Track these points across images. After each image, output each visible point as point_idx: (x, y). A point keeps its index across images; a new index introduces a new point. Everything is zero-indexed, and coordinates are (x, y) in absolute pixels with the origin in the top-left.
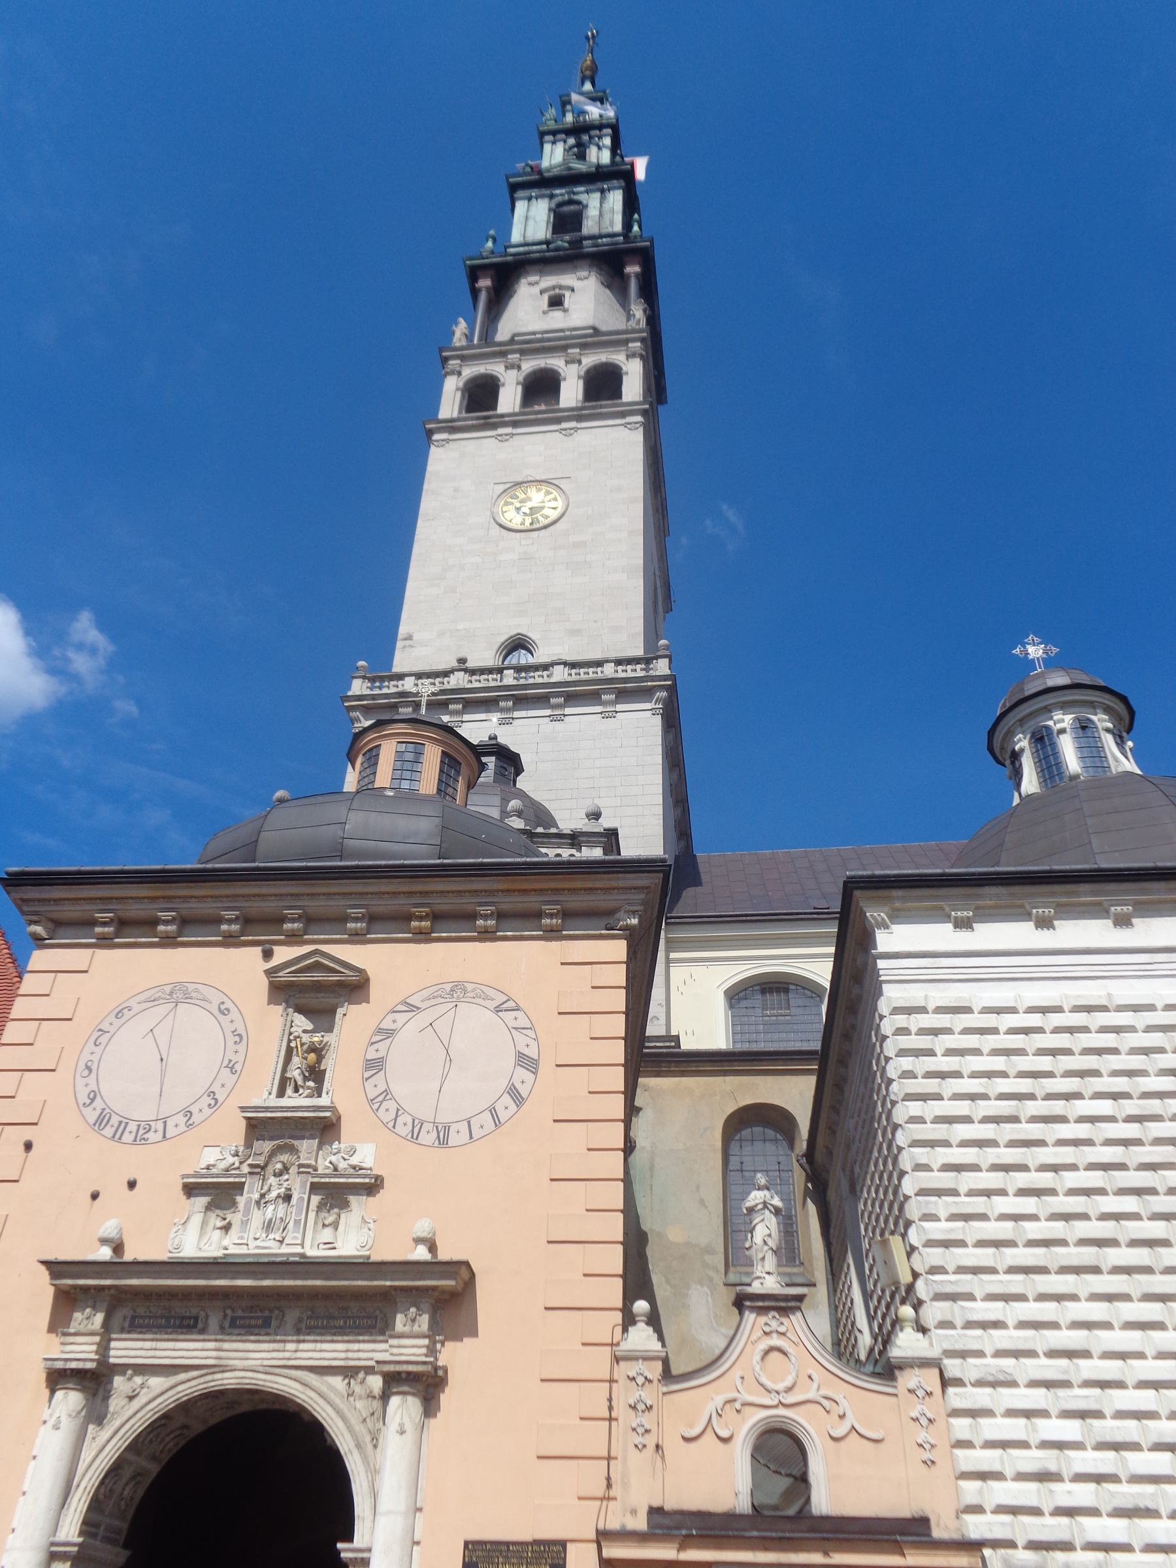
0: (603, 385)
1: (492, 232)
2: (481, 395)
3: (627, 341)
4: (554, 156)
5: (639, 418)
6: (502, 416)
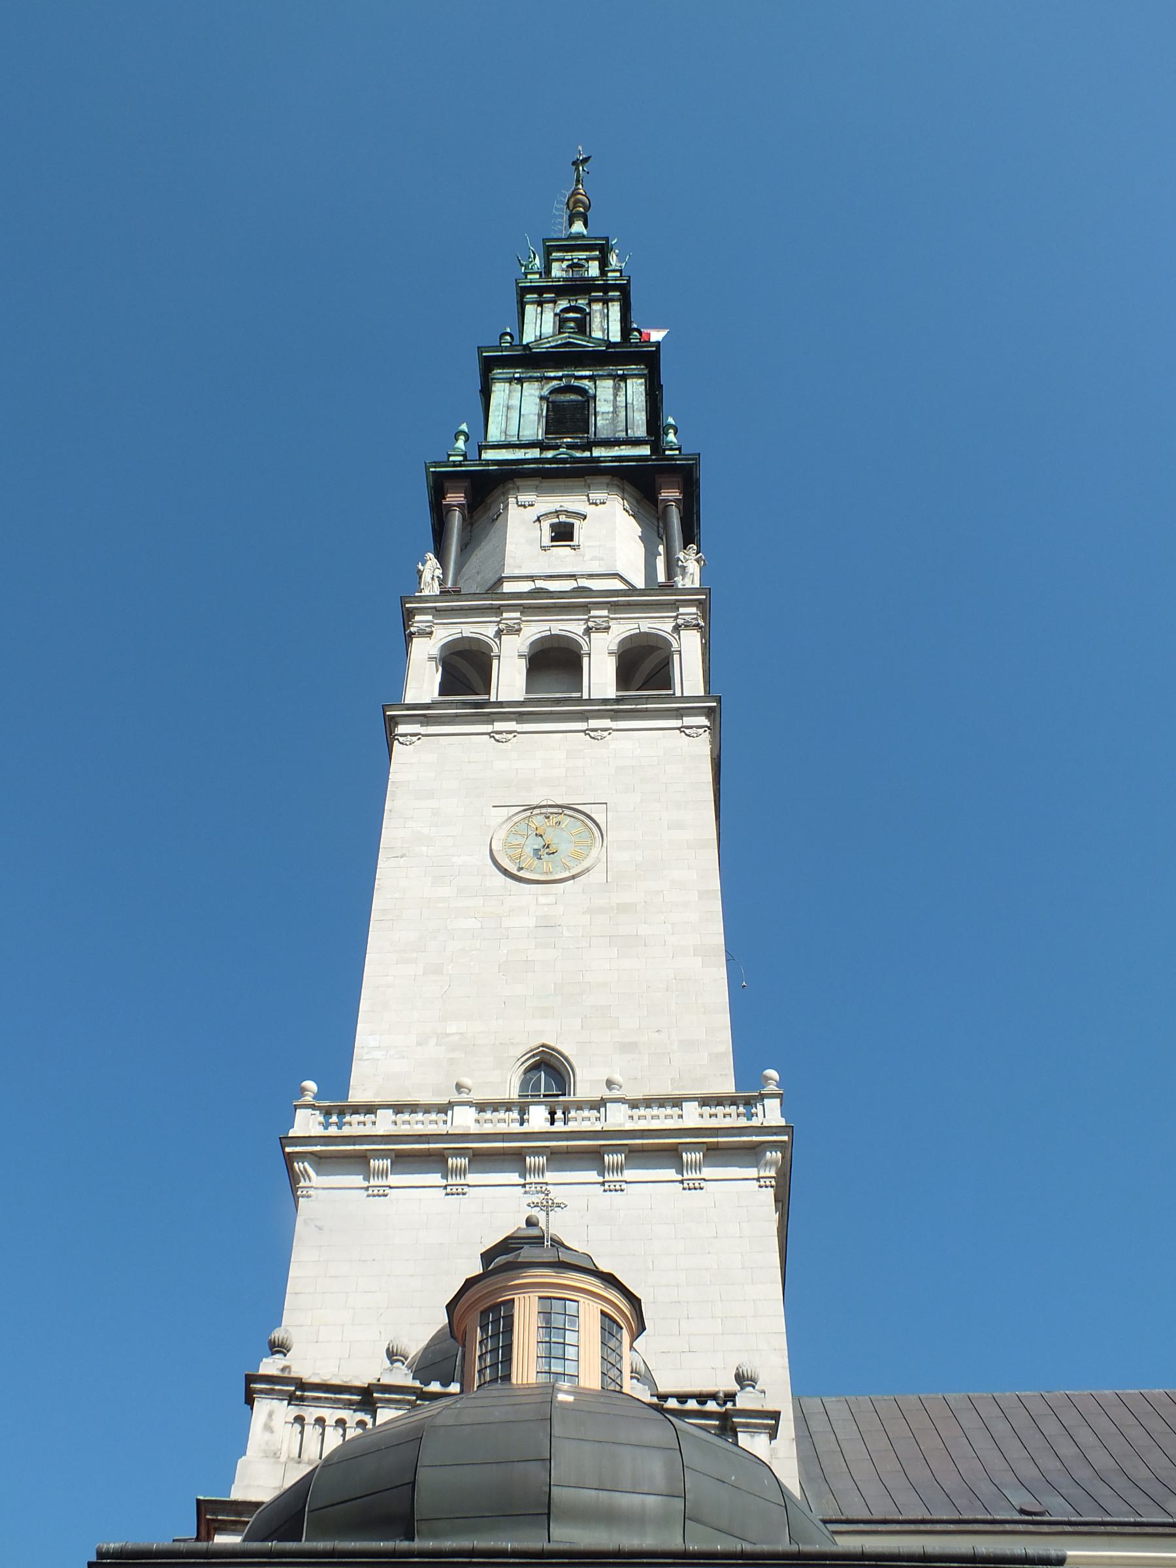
0: (644, 667)
1: (464, 427)
2: (466, 670)
3: (675, 606)
4: (540, 325)
5: (703, 721)
6: (500, 704)
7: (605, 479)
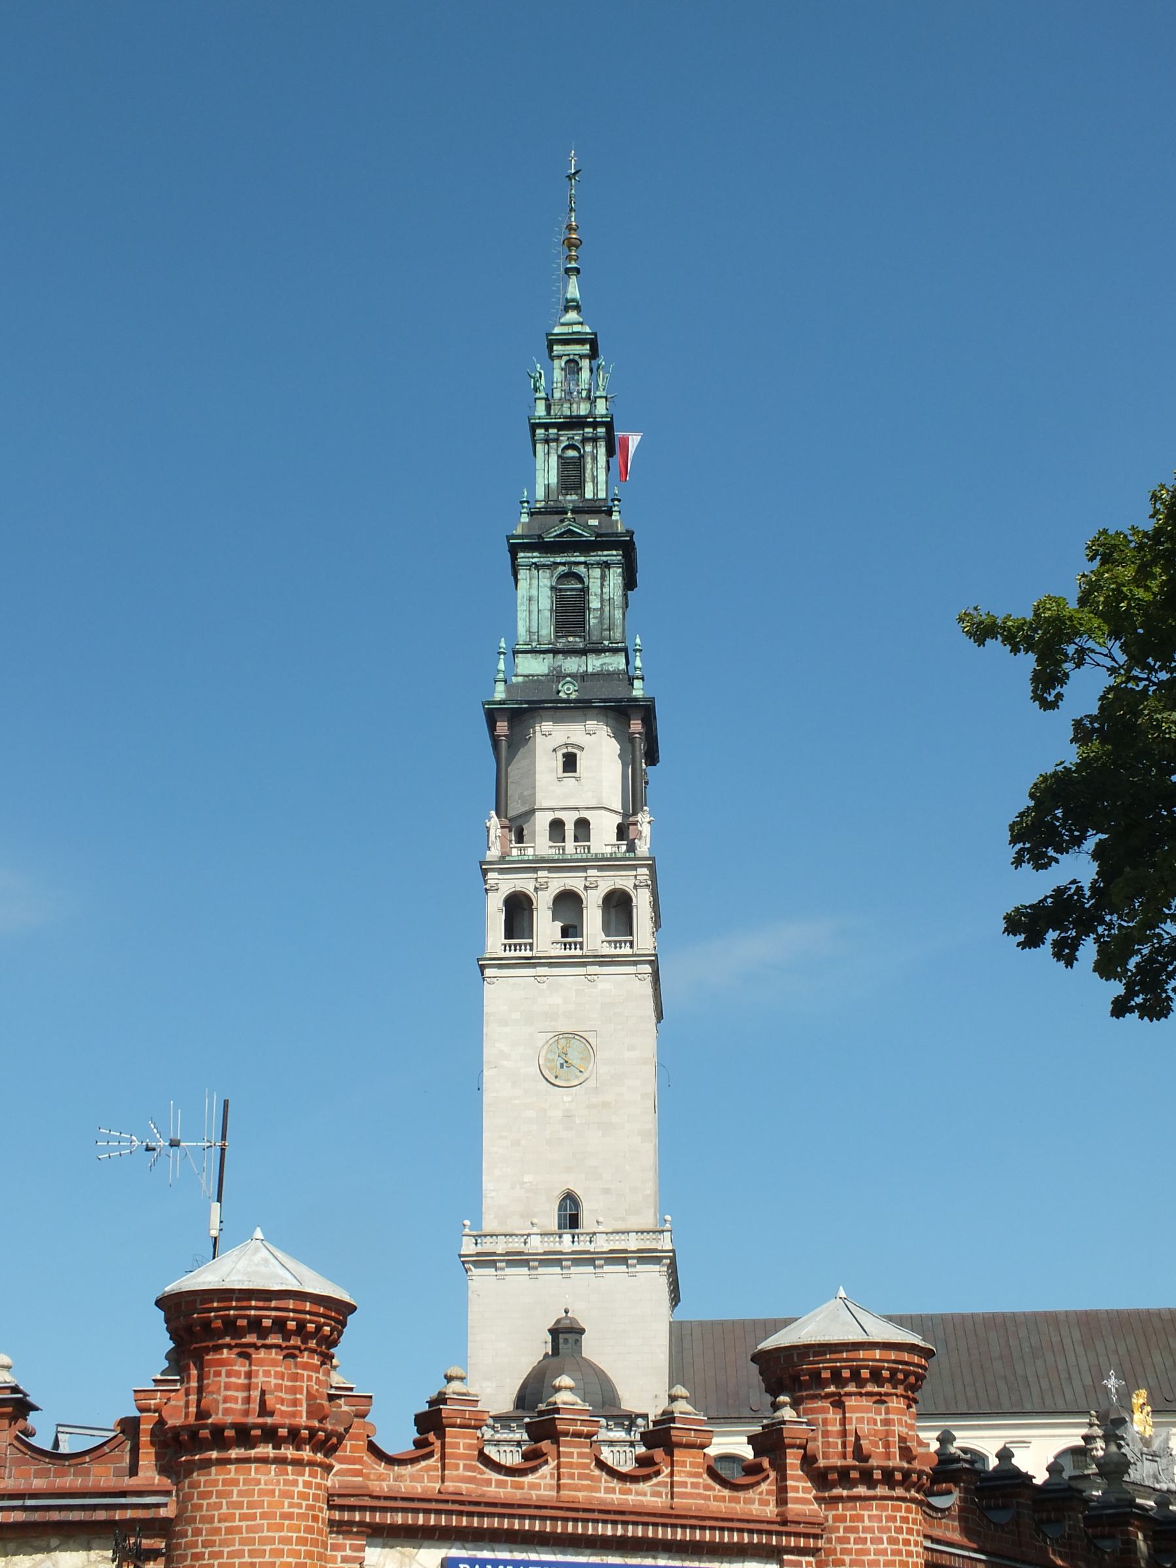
2: (518, 911)
3: (635, 867)
7: (595, 711)
